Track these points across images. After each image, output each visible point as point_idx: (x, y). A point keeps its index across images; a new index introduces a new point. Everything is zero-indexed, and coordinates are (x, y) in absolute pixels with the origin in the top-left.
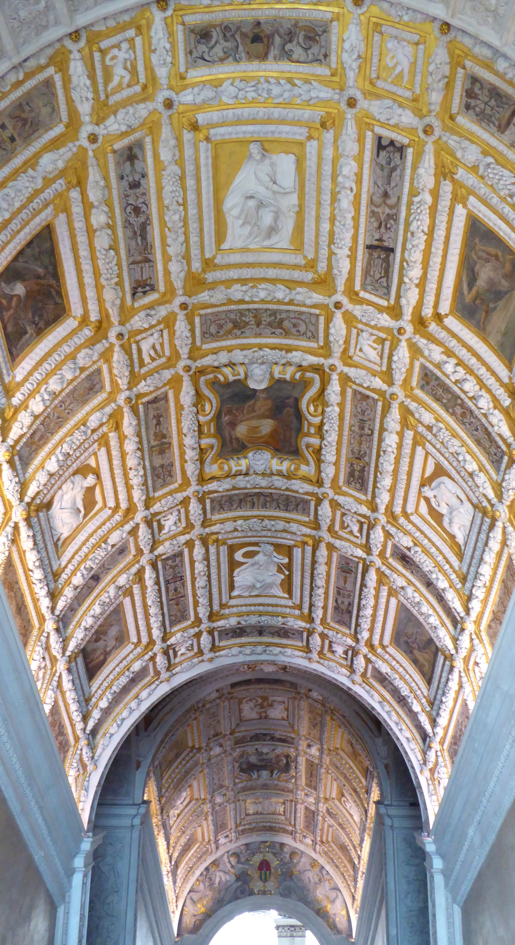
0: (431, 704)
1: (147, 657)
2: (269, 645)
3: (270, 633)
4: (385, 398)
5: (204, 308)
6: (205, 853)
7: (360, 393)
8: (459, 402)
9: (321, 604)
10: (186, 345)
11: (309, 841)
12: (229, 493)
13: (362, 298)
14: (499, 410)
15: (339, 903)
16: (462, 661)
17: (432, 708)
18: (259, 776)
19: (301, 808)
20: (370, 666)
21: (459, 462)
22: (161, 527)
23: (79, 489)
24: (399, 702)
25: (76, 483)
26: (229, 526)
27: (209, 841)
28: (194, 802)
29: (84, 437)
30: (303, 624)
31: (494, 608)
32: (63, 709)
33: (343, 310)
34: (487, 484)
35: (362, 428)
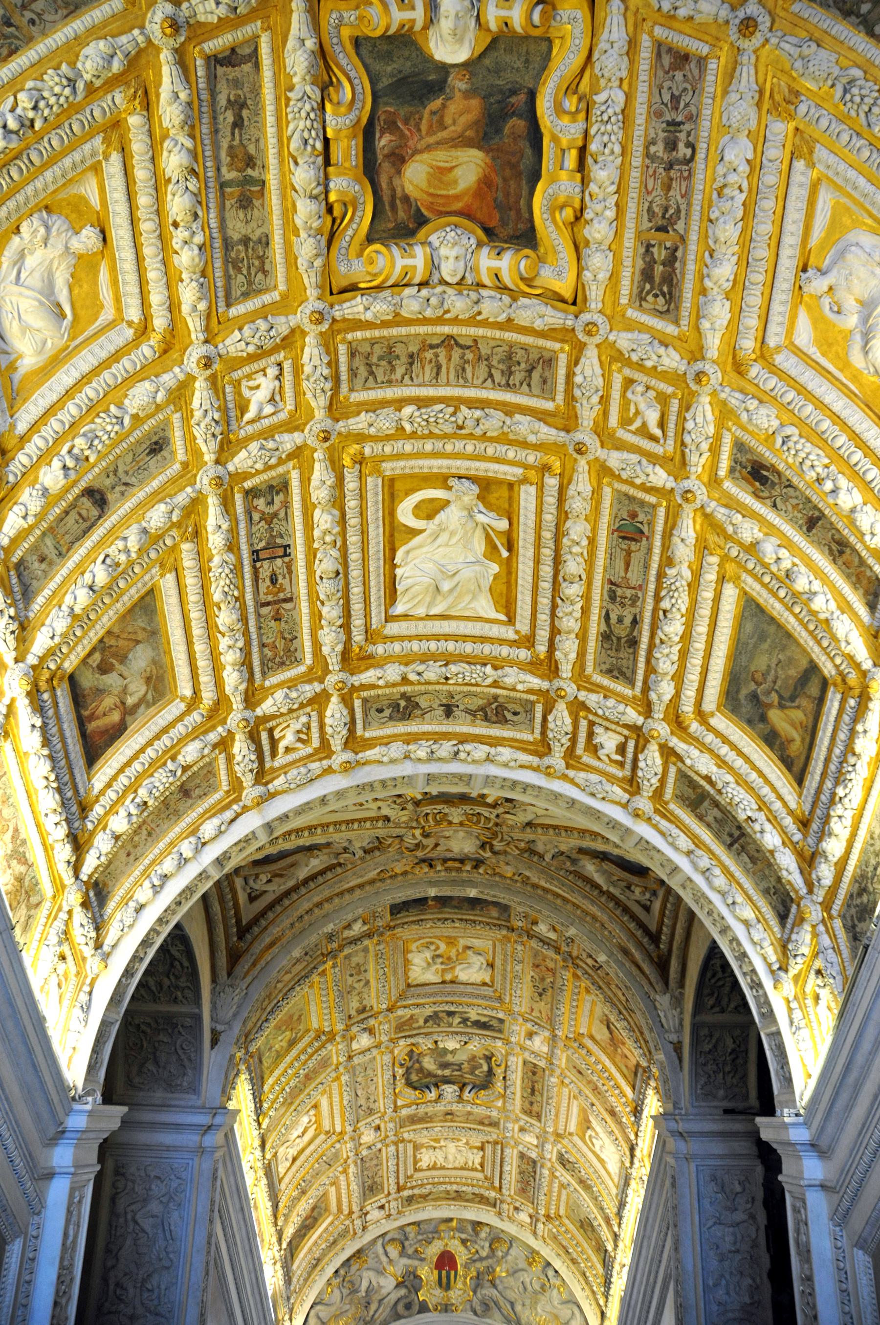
1: (213, 737)
2: (464, 739)
3: (468, 711)
6: (343, 1234)
11: (524, 1217)
17: (805, 837)
19: (512, 1155)
20: (673, 770)
23: (60, 248)
24: (730, 846)
27: (351, 1213)
28: (323, 1137)
30: (536, 682)
35: (671, 145)
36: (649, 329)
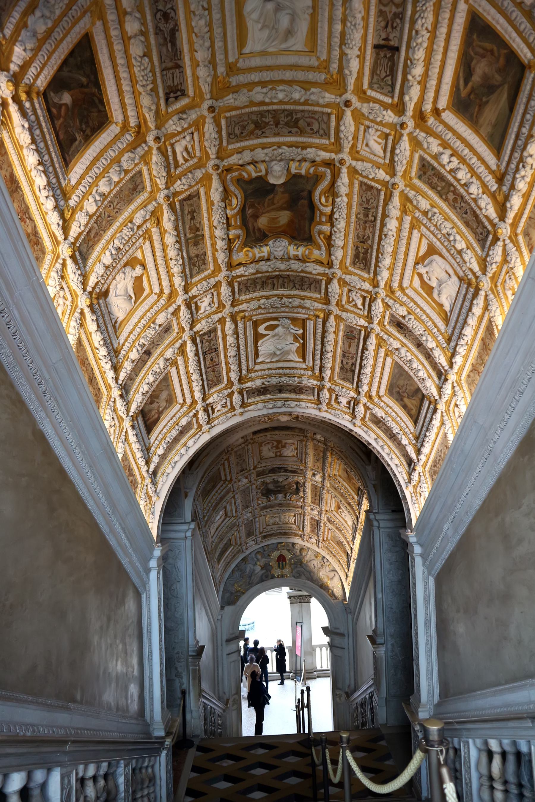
0: (417, 438)
1: (191, 414)
2: (286, 400)
3: (288, 390)
4: (387, 188)
5: (229, 111)
7: (365, 184)
8: (452, 188)
9: (329, 366)
10: (214, 146)
11: (313, 540)
12: (253, 277)
13: (370, 96)
14: (487, 195)
15: (336, 579)
16: (444, 404)
17: (417, 441)
18: (276, 498)
19: (308, 519)
20: (368, 412)
21: (450, 241)
22: (198, 308)
23: (130, 278)
24: (390, 438)
25: (127, 274)
26: (254, 305)
28: (228, 519)
29: (131, 233)
30: (315, 382)
31: (473, 361)
32: (130, 456)
33: (352, 108)
34: (474, 260)
35: (367, 215)
36: (357, 274)
